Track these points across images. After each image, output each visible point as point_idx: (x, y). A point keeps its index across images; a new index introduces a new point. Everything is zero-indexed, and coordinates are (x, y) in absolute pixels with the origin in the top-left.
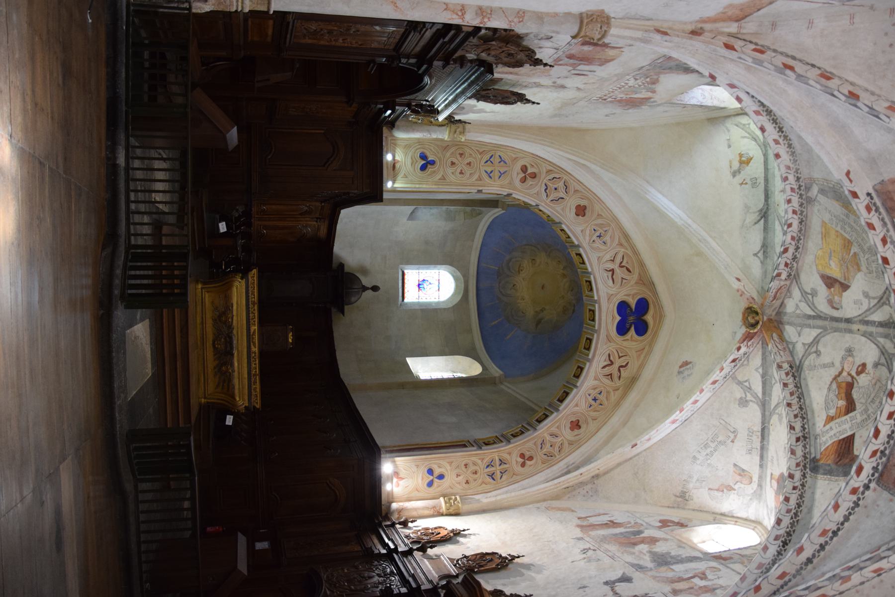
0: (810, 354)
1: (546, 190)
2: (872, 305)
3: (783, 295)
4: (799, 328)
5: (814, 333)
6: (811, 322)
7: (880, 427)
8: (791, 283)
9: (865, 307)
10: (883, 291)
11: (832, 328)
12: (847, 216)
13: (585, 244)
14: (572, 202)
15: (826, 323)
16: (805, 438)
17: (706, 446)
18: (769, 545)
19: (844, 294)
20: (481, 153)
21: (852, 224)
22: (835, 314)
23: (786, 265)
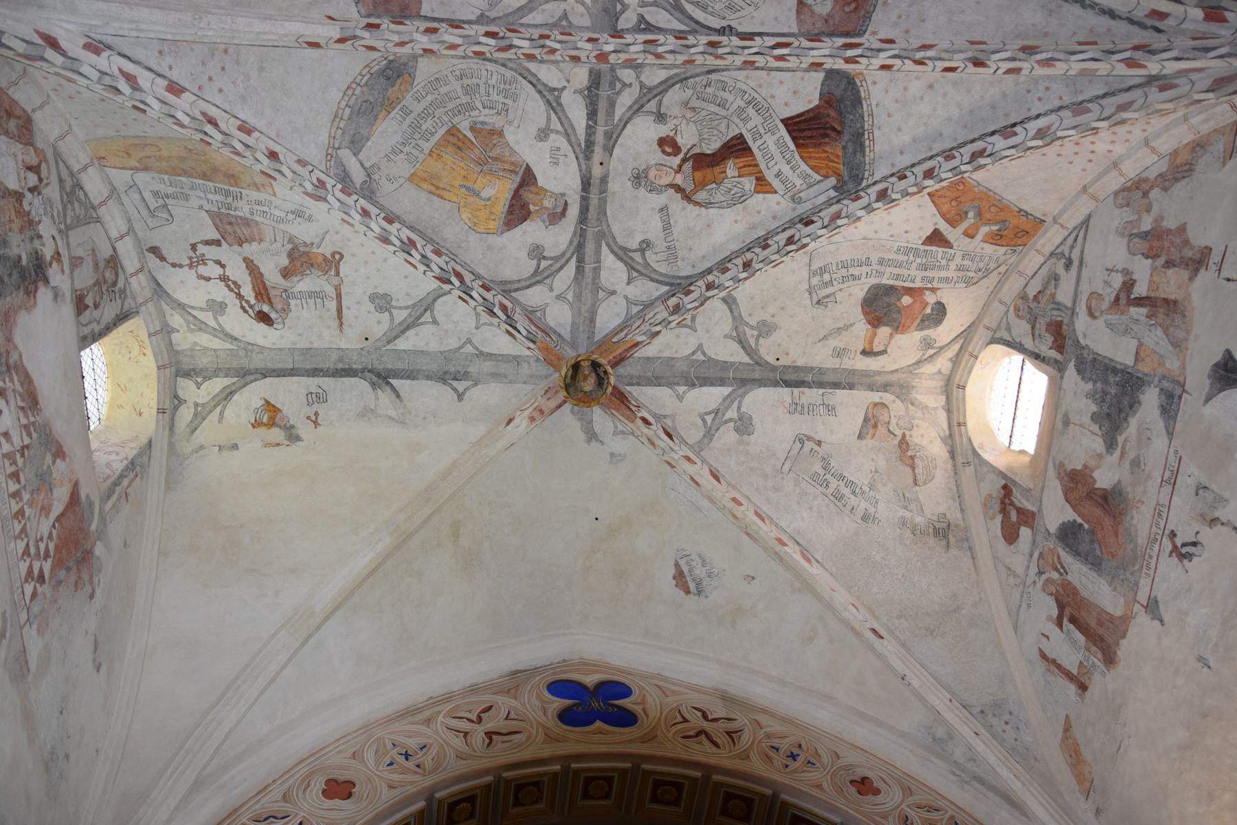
0: (647, 265)
2: (559, 128)
4: (601, 294)
6: (588, 268)
9: (562, 142)
10: (538, 96)
15: (590, 233)
17: (838, 497)
22: (574, 211)
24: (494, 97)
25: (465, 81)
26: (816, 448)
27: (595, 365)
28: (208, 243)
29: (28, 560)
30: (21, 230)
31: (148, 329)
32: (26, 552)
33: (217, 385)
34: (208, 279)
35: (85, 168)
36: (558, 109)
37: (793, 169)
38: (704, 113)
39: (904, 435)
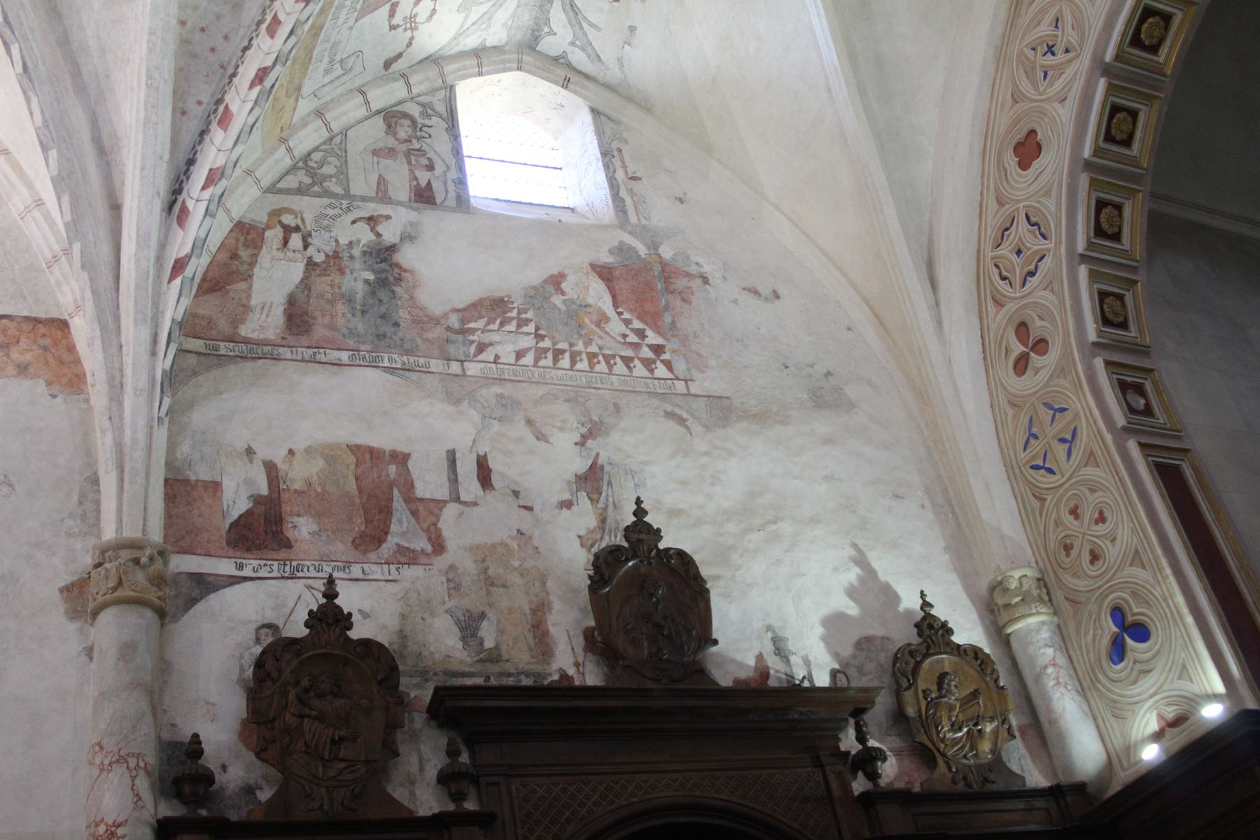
1: (1031, 274)
13: (1084, 63)
14: (1025, 186)
20: (1042, 500)
28: (392, 14)
29: (637, 362)
30: (342, 272)
31: (472, 75)
32: (627, 361)
34: (434, 10)
35: (289, 150)
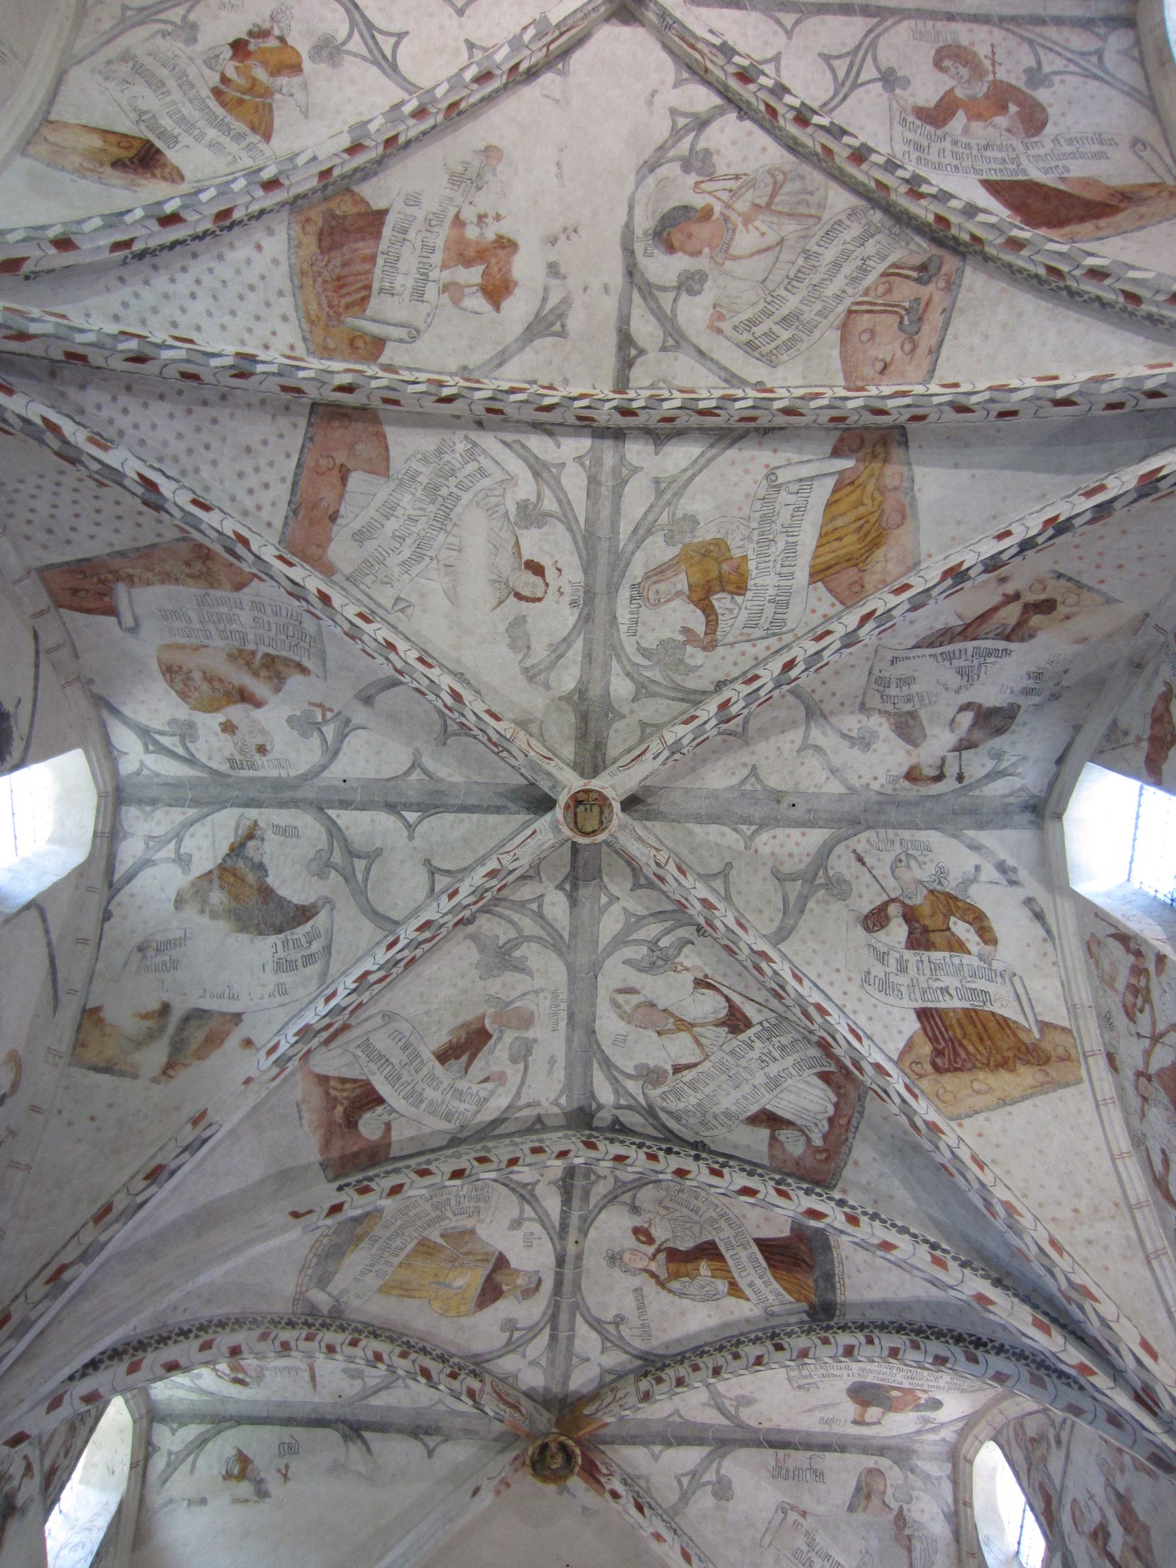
0: (621, 1338)
2: (533, 1215)
3: (511, 1391)
4: (575, 1360)
5: (582, 1328)
6: (562, 1335)
7: (737, 1188)
8: (490, 1373)
9: (536, 1228)
10: (510, 1193)
11: (574, 1294)
12: (375, 1240)
15: (565, 1303)
16: (774, 1336)
18: (991, 1372)
19: (513, 1264)
21: (389, 1232)
22: (548, 1285)
23: (453, 1376)
24: (466, 1203)
25: (435, 1200)
26: (800, 1520)
27: (563, 1447)
33: (191, 1432)
36: (532, 1200)
37: (766, 1284)
38: (677, 1214)
39: (901, 1509)
